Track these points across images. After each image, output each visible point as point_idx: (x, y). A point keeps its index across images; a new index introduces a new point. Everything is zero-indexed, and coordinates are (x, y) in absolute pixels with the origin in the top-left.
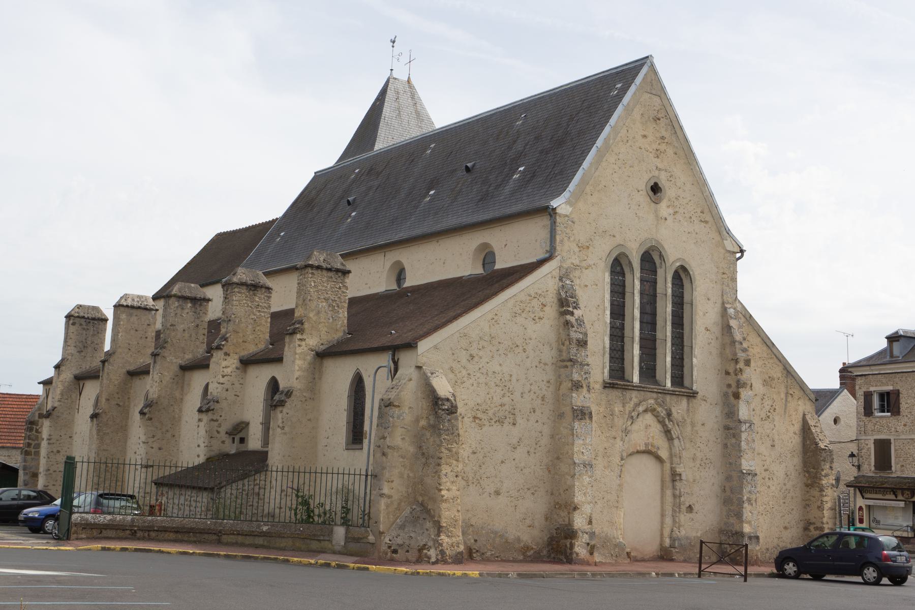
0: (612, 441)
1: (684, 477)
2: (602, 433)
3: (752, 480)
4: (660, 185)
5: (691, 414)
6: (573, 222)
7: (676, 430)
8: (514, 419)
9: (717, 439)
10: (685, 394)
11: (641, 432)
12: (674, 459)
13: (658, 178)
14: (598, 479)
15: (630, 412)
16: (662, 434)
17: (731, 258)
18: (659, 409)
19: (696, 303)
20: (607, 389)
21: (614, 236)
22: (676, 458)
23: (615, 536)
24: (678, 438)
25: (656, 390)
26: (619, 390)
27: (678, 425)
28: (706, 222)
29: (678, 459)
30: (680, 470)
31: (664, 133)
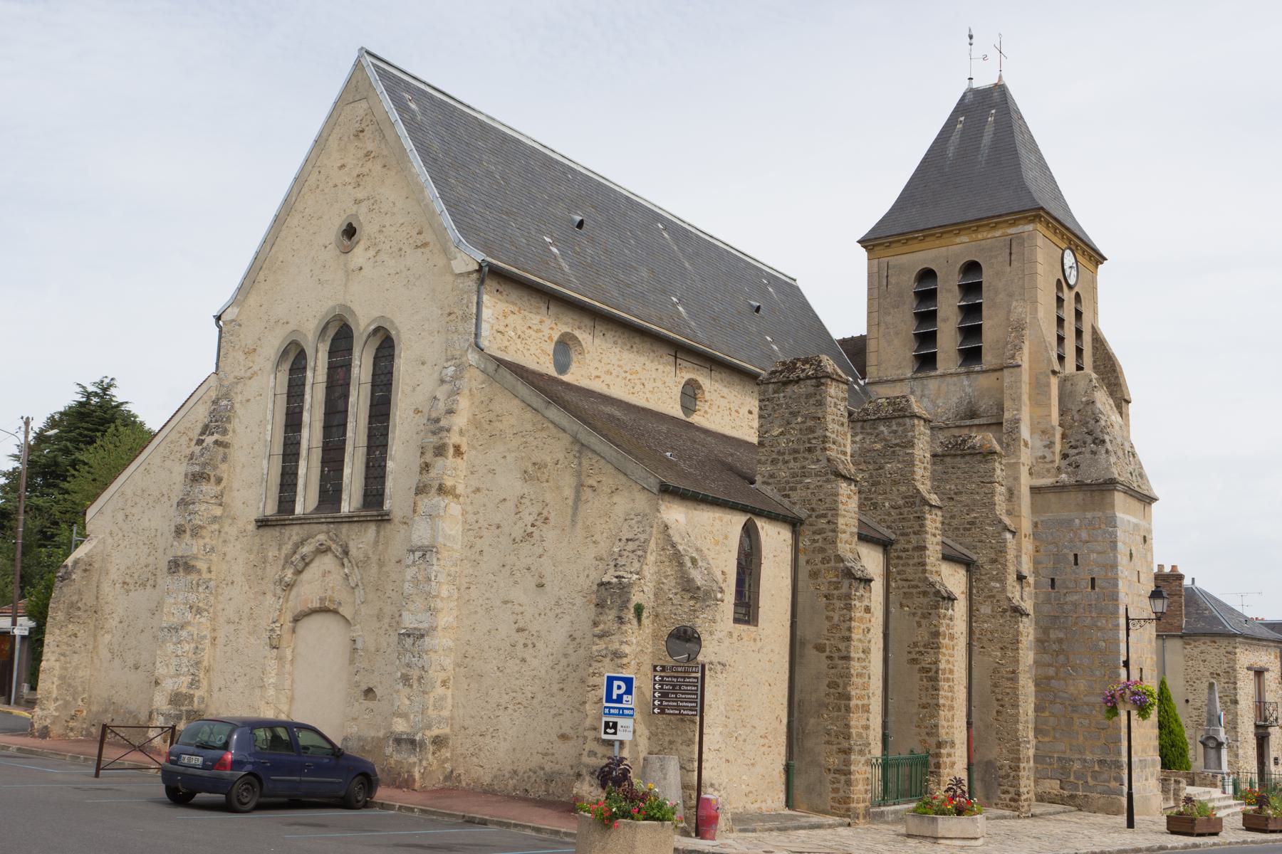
5: (381, 547)
6: (240, 325)
8: (155, 581)
10: (369, 519)
13: (356, 216)
25: (323, 520)
26: (277, 528)
27: (358, 567)
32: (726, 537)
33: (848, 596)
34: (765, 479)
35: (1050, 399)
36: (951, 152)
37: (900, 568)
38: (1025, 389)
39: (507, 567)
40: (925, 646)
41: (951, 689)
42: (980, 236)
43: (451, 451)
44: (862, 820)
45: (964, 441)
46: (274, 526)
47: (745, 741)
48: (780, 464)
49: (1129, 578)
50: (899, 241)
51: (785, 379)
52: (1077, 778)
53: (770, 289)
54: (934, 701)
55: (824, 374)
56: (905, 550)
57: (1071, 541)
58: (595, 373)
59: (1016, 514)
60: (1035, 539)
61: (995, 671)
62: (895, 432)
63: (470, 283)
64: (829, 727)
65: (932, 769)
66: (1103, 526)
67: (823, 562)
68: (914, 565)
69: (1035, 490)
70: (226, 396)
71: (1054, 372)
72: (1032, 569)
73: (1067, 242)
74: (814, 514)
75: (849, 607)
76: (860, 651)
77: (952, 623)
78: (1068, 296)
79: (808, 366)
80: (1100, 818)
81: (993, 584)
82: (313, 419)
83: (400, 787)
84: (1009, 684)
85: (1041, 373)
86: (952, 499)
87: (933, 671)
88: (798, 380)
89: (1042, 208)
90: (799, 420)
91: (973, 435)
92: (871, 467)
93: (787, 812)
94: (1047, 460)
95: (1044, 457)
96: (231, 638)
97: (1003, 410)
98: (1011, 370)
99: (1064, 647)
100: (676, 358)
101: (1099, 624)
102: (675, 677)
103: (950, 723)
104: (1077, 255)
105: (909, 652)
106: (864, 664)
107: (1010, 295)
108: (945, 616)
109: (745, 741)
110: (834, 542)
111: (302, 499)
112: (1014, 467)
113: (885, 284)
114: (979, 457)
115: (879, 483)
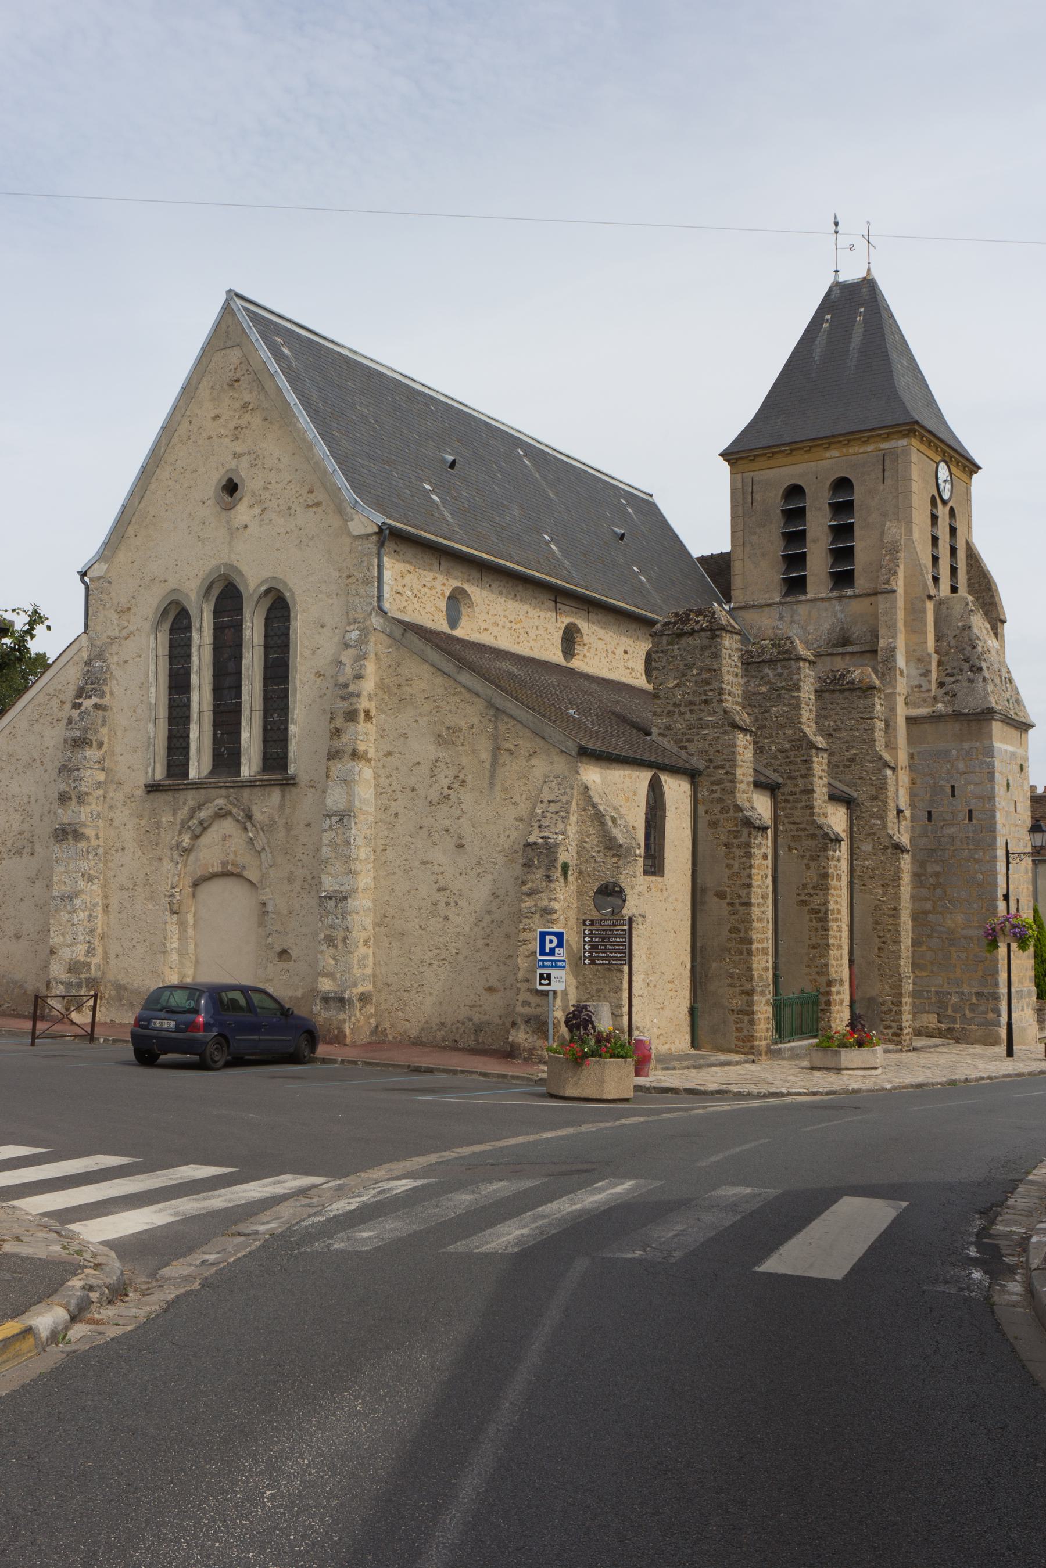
3: (336, 906)
5: (287, 811)
6: (110, 583)
8: (32, 848)
13: (236, 471)
14: (137, 915)
25: (222, 785)
26: (170, 793)
27: (263, 831)
30: (264, 898)
31: (247, 397)
32: (635, 794)
33: (748, 845)
34: (661, 731)
35: (925, 625)
36: (817, 354)
37: (788, 811)
38: (901, 615)
39: (424, 829)
40: (814, 888)
41: (840, 930)
42: (851, 451)
43: (362, 716)
44: (764, 1057)
45: (843, 676)
46: (166, 790)
47: (655, 986)
48: (676, 716)
49: (1006, 809)
50: (765, 455)
51: (679, 631)
52: (954, 1011)
53: (630, 510)
54: (824, 941)
55: (719, 626)
56: (792, 794)
57: (948, 772)
58: (485, 626)
59: (893, 746)
60: (911, 770)
61: (877, 908)
62: (780, 675)
63: (370, 546)
64: (731, 971)
65: (823, 1007)
66: (980, 757)
67: (721, 812)
68: (802, 808)
69: (911, 721)
71: (930, 597)
72: (908, 802)
73: (941, 454)
74: (712, 765)
75: (749, 855)
76: (760, 896)
77: (839, 864)
78: (942, 512)
79: (701, 618)
80: (978, 1049)
81: (874, 821)
82: (202, 681)
84: (890, 921)
85: (916, 598)
86: (832, 735)
87: (823, 912)
88: (692, 633)
89: (917, 422)
90: (695, 672)
91: (852, 669)
92: (756, 710)
93: (693, 1052)
94: (923, 689)
95: (920, 686)
97: (877, 637)
98: (886, 595)
99: (941, 881)
100: (556, 602)
101: (976, 856)
102: (603, 930)
103: (838, 962)
104: (951, 466)
105: (798, 894)
106: (763, 909)
107: (884, 515)
108: (833, 857)
109: (655, 986)
110: (732, 793)
111: (196, 764)
112: (891, 698)
113: (750, 501)
114: (858, 693)
115: (765, 727)
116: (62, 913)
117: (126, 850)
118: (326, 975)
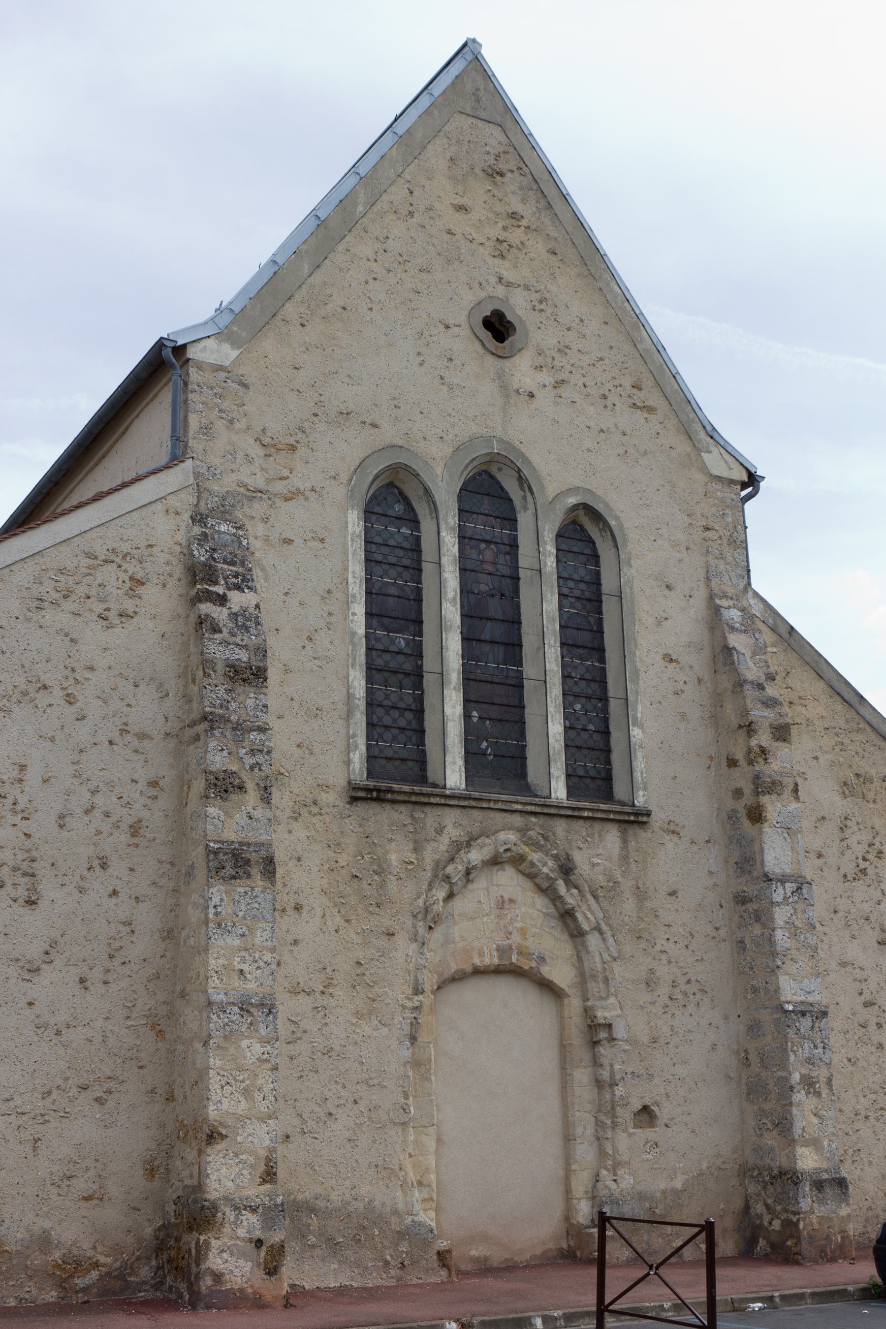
0: (383, 942)
1: (620, 1032)
2: (347, 921)
3: (812, 1027)
4: (509, 317)
5: (633, 866)
6: (245, 386)
7: (590, 909)
9: (717, 929)
10: (612, 816)
11: (485, 919)
12: (591, 985)
13: (506, 301)
14: (337, 1048)
15: (438, 866)
16: (553, 923)
17: (726, 495)
18: (535, 857)
19: (632, 593)
20: (359, 804)
21: (375, 426)
22: (596, 981)
23: (401, 1206)
24: (598, 929)
26: (402, 808)
27: (596, 897)
28: (651, 410)
29: (601, 985)
30: (607, 1014)
31: (516, 205)
39: (840, 914)
46: (393, 802)
70: (224, 512)
83: (833, 1260)
96: (304, 1025)
116: (244, 1043)
117: (305, 911)
118: (806, 1144)
